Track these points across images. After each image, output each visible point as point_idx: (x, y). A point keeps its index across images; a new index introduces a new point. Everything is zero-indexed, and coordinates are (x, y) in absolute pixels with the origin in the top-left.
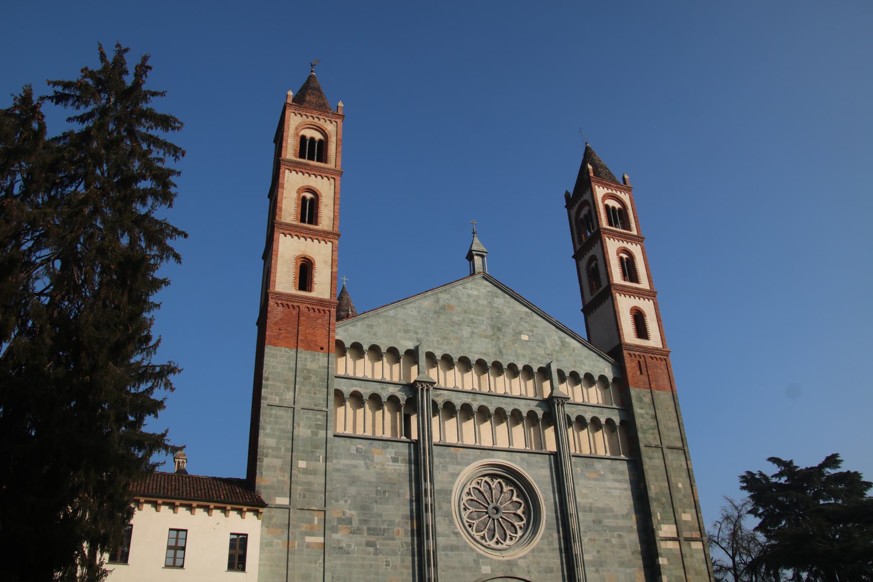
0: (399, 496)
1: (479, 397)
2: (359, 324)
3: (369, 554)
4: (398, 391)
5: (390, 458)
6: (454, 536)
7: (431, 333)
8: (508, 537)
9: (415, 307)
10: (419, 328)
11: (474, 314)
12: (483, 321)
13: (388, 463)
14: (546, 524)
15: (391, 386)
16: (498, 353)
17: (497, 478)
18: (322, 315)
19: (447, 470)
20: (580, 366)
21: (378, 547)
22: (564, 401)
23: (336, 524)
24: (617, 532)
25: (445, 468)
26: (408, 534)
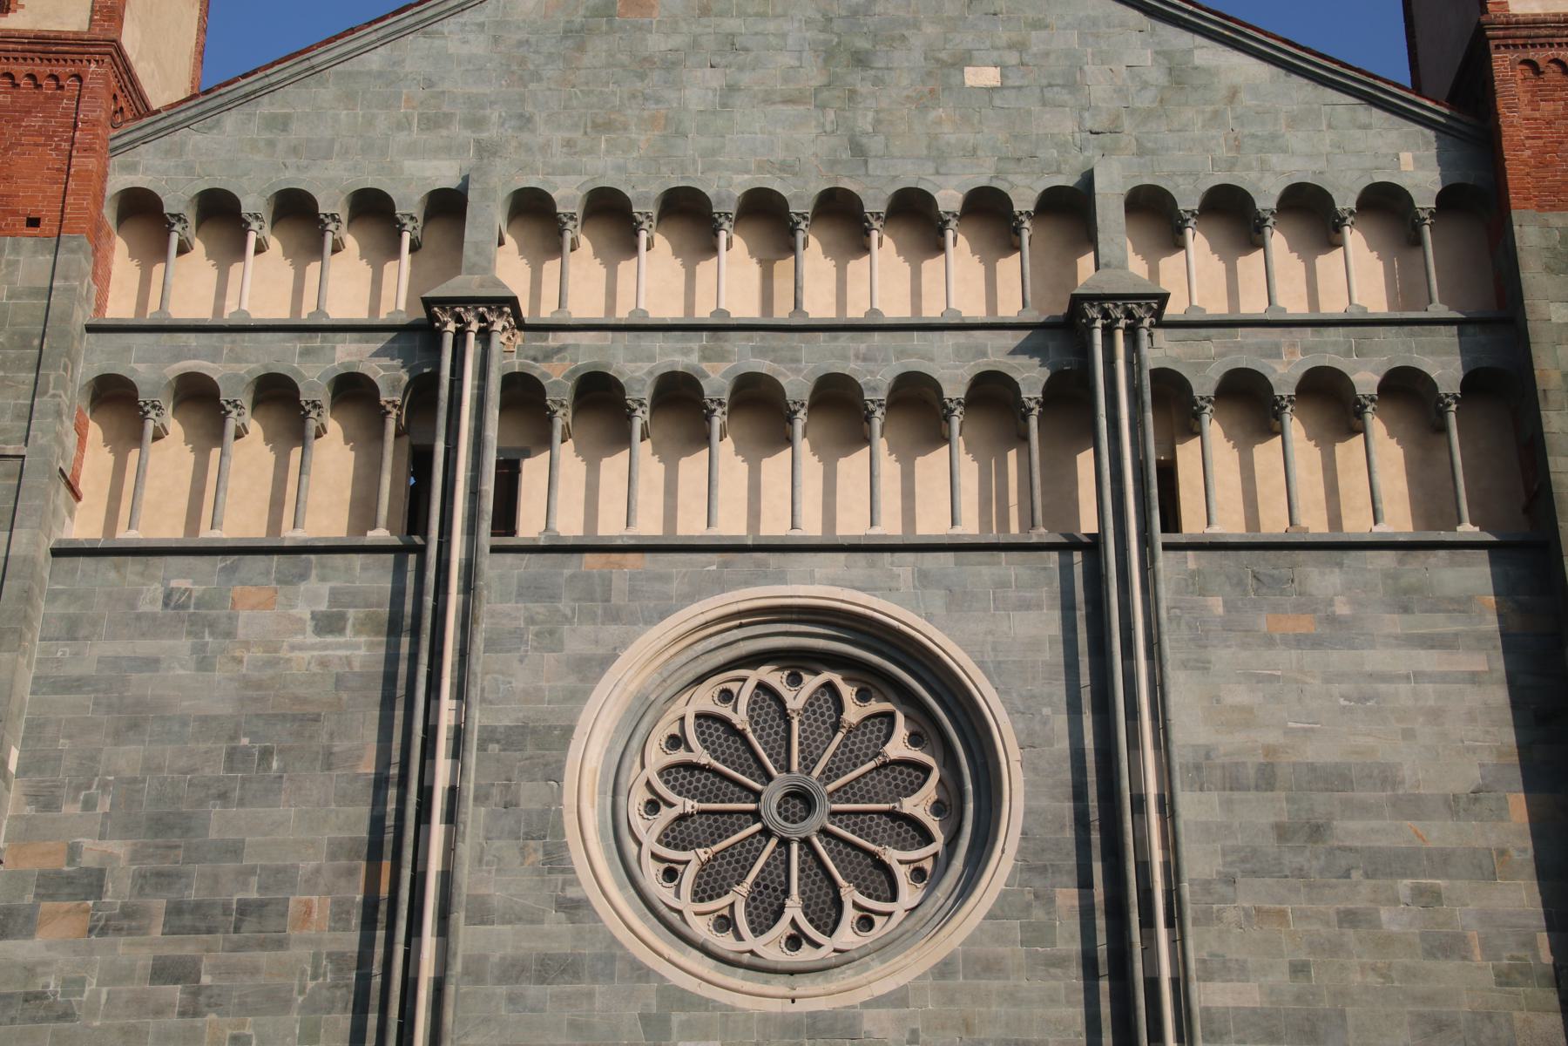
0: (328, 766)
1: (736, 341)
2: (230, 120)
3: (159, 1012)
4: (377, 354)
5: (309, 616)
6: (562, 916)
7: (539, 119)
8: (850, 915)
9: (481, 25)
10: (492, 103)
11: (742, 14)
12: (784, 36)
13: (299, 639)
14: (1020, 851)
15: (344, 341)
16: (846, 155)
17: (817, 666)
18: (48, 98)
19: (557, 647)
20: (1262, 162)
21: (206, 979)
22: (1139, 312)
23: (29, 898)
24: (1413, 876)
25: (549, 638)
26: (348, 921)
